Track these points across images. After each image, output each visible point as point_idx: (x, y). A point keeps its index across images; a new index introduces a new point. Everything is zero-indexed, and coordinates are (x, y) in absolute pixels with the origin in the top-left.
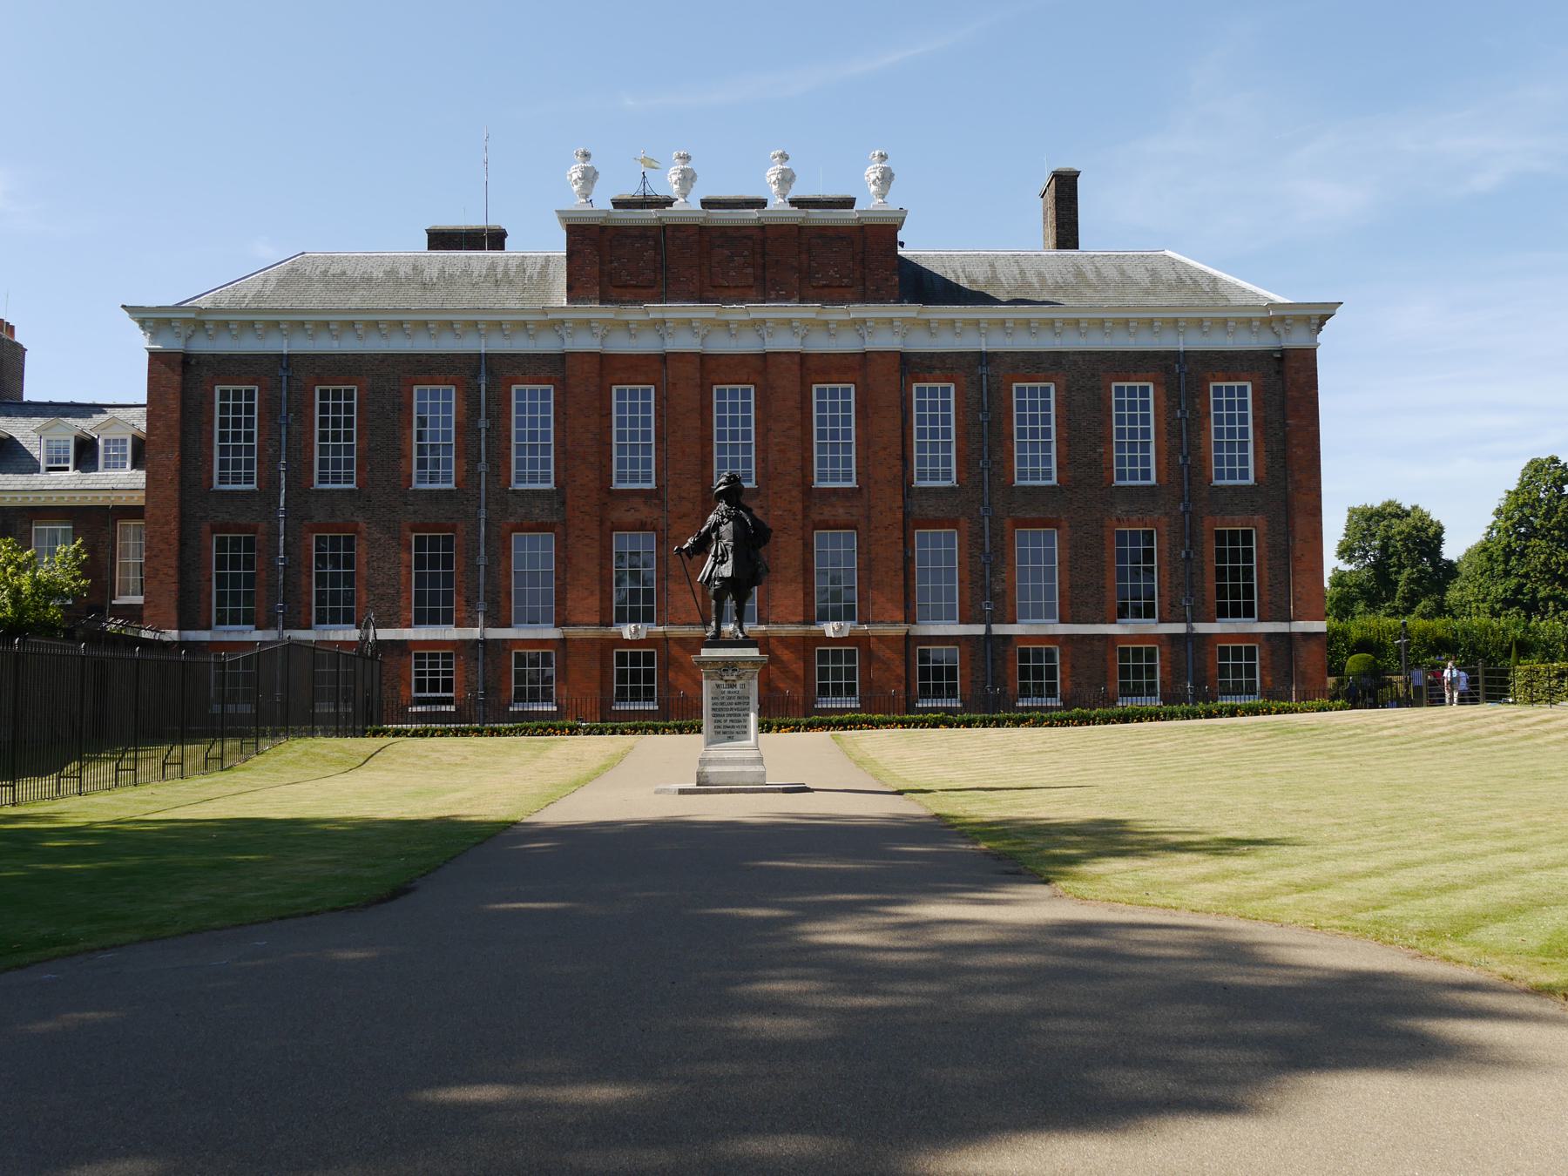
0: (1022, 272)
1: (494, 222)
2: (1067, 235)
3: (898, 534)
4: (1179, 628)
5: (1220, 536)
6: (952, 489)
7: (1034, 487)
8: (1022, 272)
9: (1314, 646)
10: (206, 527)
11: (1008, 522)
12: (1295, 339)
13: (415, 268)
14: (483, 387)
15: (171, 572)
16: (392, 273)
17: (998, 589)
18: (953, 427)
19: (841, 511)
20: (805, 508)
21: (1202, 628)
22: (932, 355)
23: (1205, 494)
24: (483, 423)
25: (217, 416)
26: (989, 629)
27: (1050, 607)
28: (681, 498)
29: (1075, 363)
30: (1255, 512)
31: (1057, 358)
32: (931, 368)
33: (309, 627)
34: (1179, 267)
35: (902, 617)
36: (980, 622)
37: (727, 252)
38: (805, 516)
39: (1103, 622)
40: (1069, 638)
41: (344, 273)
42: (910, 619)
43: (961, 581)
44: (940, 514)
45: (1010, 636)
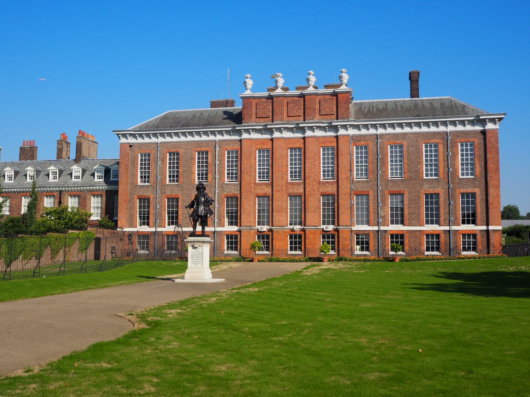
0: (396, 106)
1: (230, 98)
2: (414, 92)
3: (348, 196)
4: (447, 228)
5: (463, 195)
8: (396, 106)
9: (497, 234)
10: (136, 196)
11: (386, 192)
12: (490, 126)
13: (201, 114)
14: (217, 151)
15: (126, 210)
16: (194, 116)
17: (383, 215)
19: (330, 189)
20: (318, 188)
21: (454, 228)
23: (457, 181)
24: (217, 163)
25: (139, 162)
28: (278, 185)
29: (410, 137)
30: (475, 187)
31: (405, 134)
32: (360, 141)
33: (165, 227)
34: (453, 102)
35: (349, 224)
37: (293, 105)
38: (318, 191)
39: (420, 225)
40: (408, 231)
41: (180, 117)
42: (352, 224)
44: (363, 190)
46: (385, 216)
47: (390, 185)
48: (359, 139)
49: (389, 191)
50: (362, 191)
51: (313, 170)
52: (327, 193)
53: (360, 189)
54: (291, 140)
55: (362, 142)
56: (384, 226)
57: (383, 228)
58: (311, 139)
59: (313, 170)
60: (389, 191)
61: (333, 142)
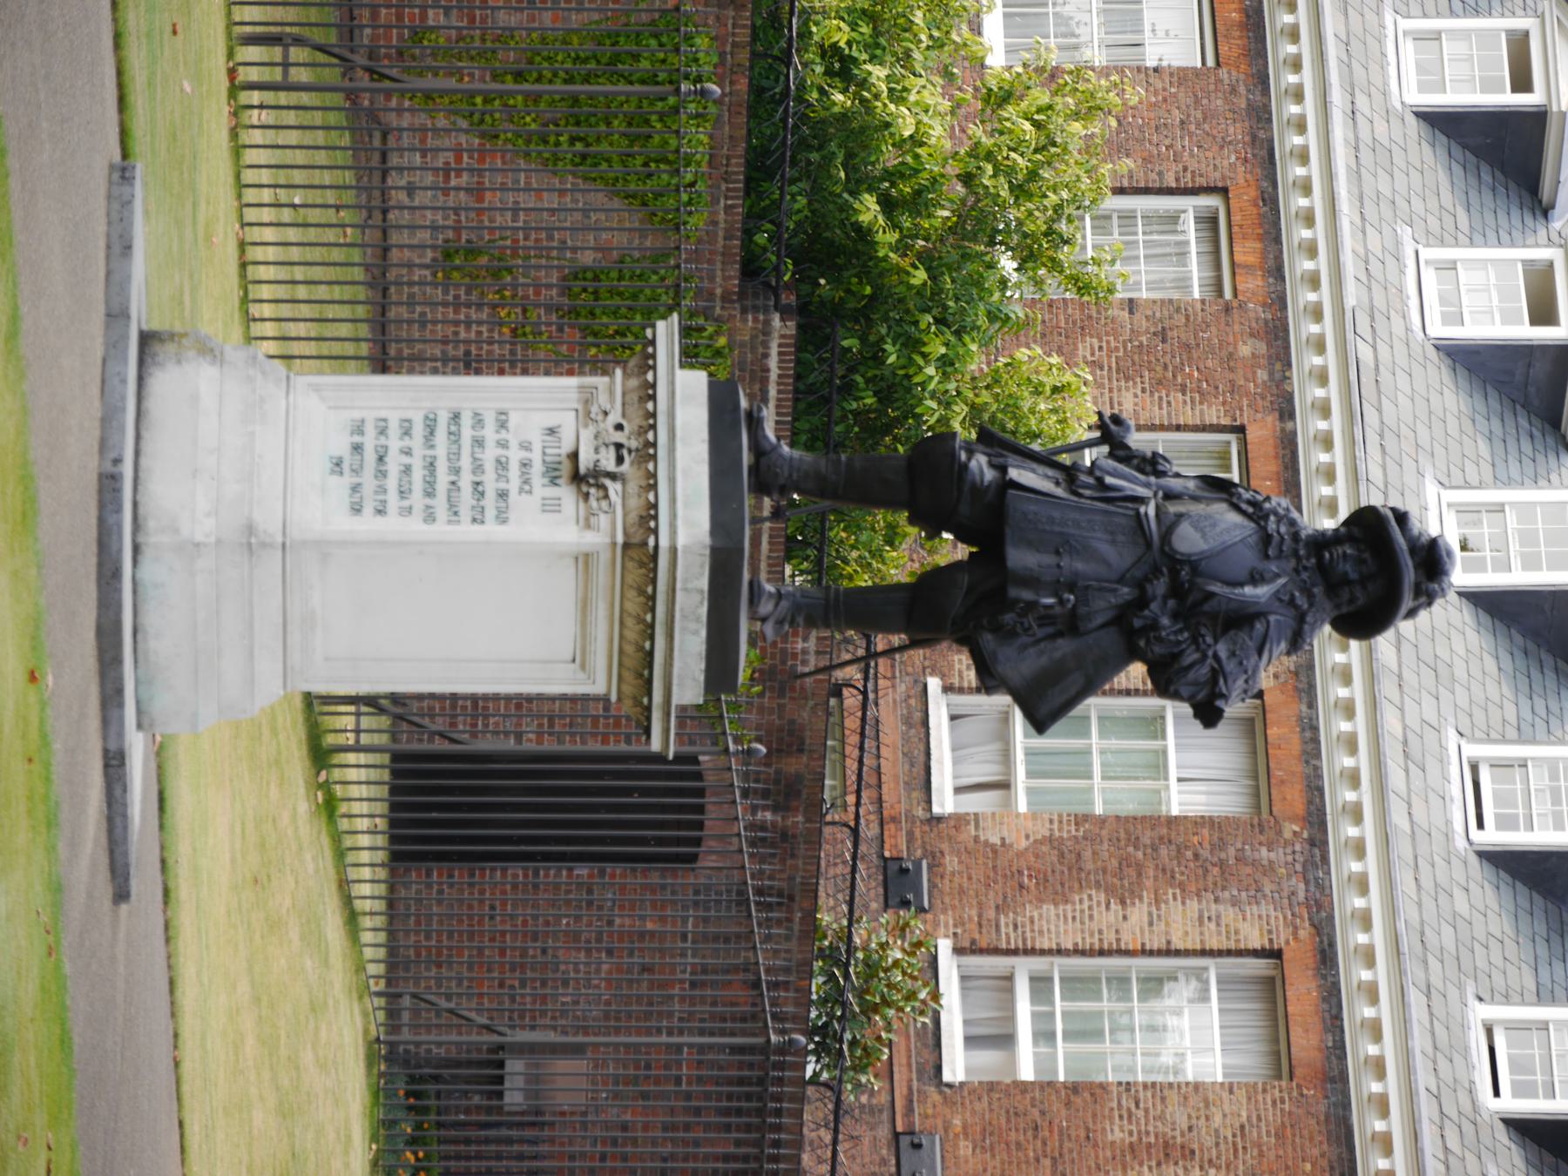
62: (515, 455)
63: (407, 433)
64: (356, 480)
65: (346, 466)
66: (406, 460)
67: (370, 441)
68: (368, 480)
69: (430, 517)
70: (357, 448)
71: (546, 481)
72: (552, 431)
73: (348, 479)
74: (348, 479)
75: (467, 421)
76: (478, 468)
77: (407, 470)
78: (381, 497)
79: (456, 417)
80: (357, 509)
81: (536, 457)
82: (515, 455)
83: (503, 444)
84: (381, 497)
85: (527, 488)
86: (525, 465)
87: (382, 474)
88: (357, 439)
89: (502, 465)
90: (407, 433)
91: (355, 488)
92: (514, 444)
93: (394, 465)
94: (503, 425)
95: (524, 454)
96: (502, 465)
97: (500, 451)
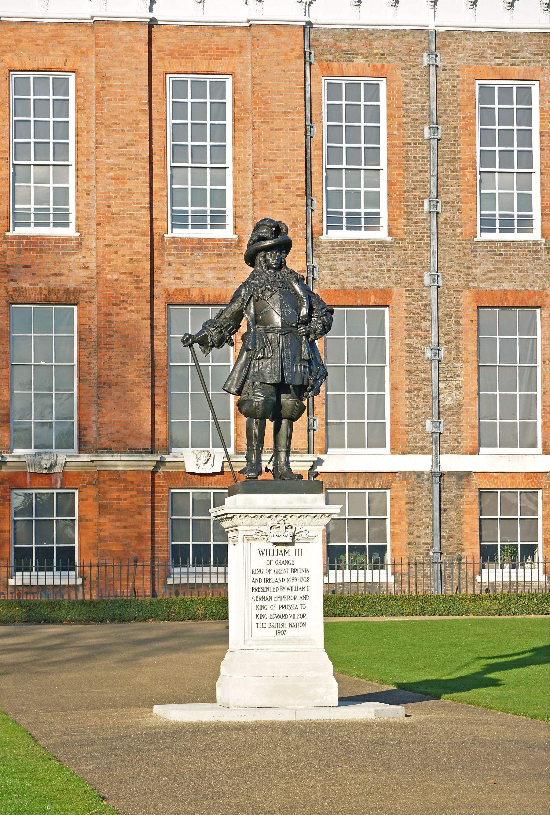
6: (382, 243)
7: (507, 244)
11: (467, 300)
18: (383, 145)
19: (210, 275)
22: (352, 33)
26: (436, 463)
27: (528, 429)
32: (350, 54)
36: (422, 451)
43: (394, 388)
44: (362, 283)
45: (469, 473)
46: (459, 404)
47: (483, 267)
48: (345, 45)
49: (478, 295)
50: (357, 291)
51: (130, 185)
52: (195, 294)
53: (350, 282)
54: (24, 30)
55: (360, 60)
56: (454, 451)
57: (450, 463)
58: (122, 32)
59: (130, 185)
60: (478, 295)
61: (226, 52)
62: (274, 566)
63: (264, 607)
64: (288, 625)
65: (281, 629)
66: (277, 607)
67: (268, 621)
68: (290, 620)
69: (307, 598)
70: (271, 625)
71: (287, 555)
72: (261, 553)
73: (288, 629)
74: (288, 629)
75: (257, 585)
76: (282, 580)
77: (283, 607)
78: (296, 616)
79: (255, 589)
80: (304, 625)
81: (274, 559)
82: (274, 566)
83: (269, 571)
84: (296, 616)
85: (290, 562)
86: (279, 563)
87: (285, 616)
88: (267, 625)
89: (279, 571)
90: (264, 607)
91: (292, 625)
92: (269, 567)
93: (277, 611)
94: (259, 571)
95: (273, 563)
96: (279, 571)
97: (272, 571)
